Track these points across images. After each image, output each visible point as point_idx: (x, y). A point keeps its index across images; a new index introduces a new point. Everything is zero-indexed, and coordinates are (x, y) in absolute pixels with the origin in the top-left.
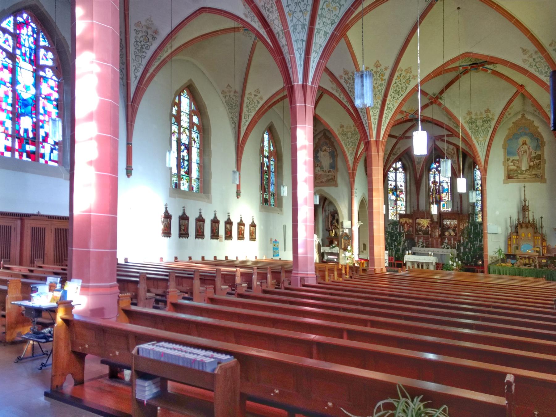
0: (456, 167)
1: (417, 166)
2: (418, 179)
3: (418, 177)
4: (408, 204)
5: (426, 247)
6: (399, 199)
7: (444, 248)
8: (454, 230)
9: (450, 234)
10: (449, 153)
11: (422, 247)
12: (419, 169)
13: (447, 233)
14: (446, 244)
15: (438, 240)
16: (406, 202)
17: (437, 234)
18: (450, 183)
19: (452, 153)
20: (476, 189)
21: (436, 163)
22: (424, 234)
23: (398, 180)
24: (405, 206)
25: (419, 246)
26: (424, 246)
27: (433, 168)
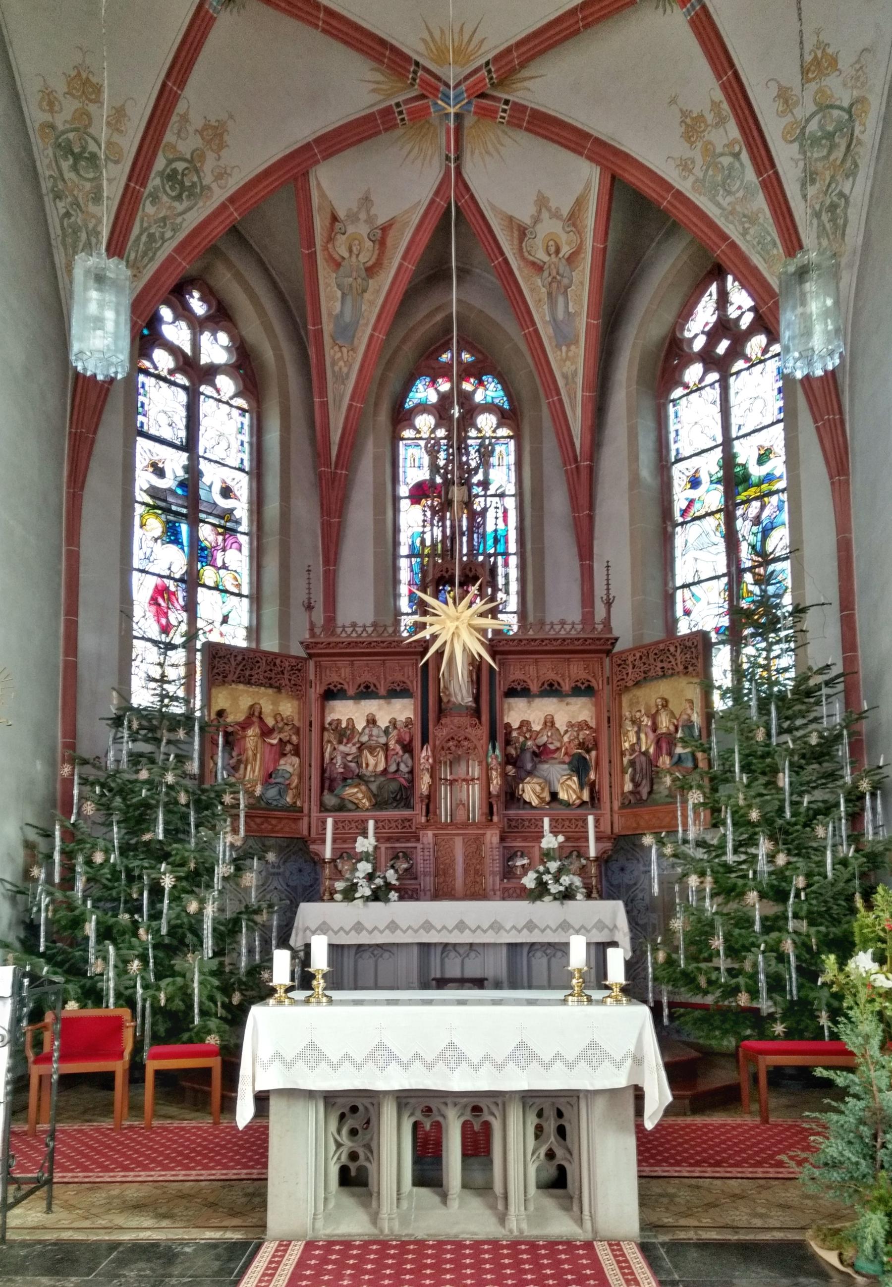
0: (568, 367)
1: (330, 352)
2: (334, 453)
3: (336, 437)
4: (271, 612)
5: (407, 894)
6: (209, 575)
7: (540, 891)
8: (579, 767)
9: (554, 796)
10: (541, 255)
11: (377, 896)
12: (344, 379)
13: (530, 791)
14: (553, 866)
15: (478, 840)
16: (256, 599)
17: (474, 794)
18: (520, 495)
19: (565, 250)
20: (684, 512)
21: (433, 382)
22: (379, 804)
23: (204, 442)
24: (249, 629)
25: (349, 894)
26: (388, 887)
27: (422, 408)
